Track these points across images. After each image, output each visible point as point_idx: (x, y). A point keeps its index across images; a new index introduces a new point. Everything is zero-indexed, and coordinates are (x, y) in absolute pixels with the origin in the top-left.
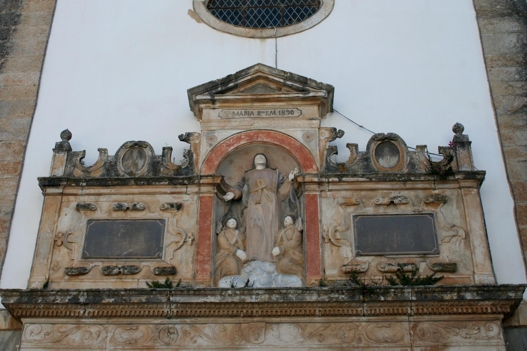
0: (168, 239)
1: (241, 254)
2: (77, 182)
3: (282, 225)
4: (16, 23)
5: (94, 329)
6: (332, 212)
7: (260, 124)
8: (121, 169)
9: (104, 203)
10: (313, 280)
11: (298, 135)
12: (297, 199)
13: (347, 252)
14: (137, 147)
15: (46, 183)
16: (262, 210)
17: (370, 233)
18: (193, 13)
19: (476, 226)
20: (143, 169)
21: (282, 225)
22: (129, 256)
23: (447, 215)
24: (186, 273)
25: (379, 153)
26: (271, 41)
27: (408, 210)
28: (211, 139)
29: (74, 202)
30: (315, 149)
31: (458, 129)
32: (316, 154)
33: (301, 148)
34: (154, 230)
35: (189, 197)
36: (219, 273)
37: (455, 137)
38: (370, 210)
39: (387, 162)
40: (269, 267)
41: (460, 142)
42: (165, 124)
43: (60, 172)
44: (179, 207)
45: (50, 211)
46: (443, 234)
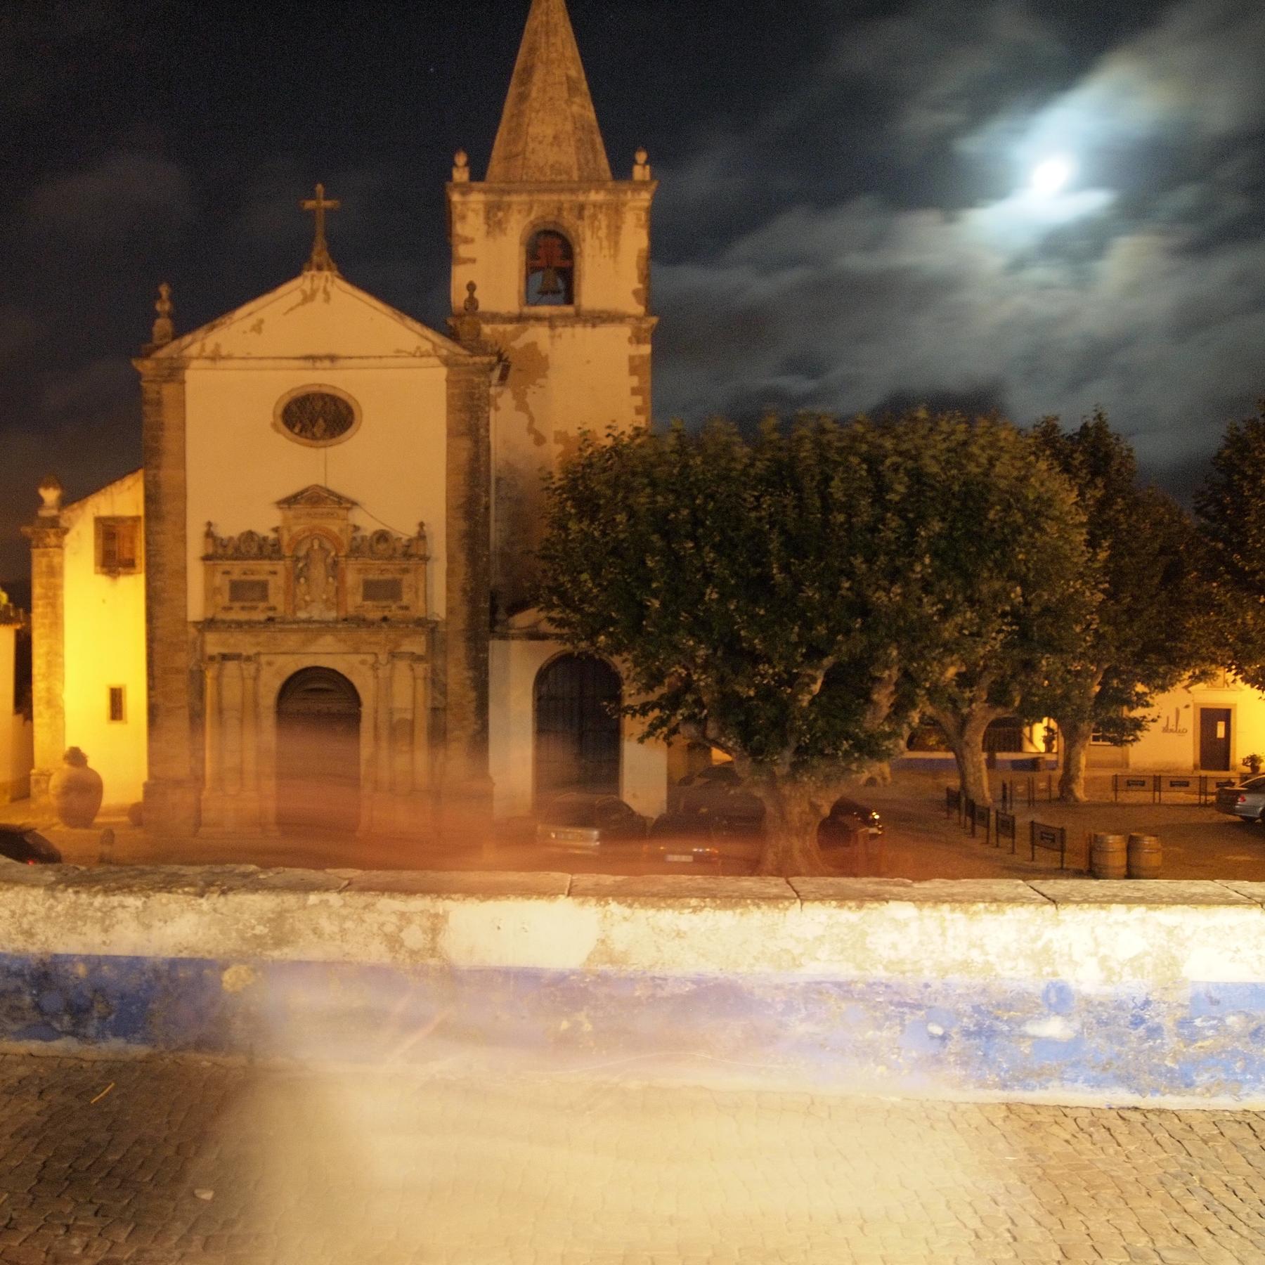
0: (272, 590)
1: (307, 598)
2: (221, 558)
3: (327, 582)
4: (162, 430)
5: (240, 637)
6: (352, 578)
7: (316, 522)
8: (243, 549)
9: (238, 569)
10: (342, 614)
11: (335, 529)
12: (335, 569)
13: (359, 599)
14: (250, 535)
15: (206, 558)
16: (318, 572)
17: (372, 590)
18: (274, 425)
19: (422, 585)
20: (255, 550)
21: (327, 582)
22: (254, 600)
23: (408, 579)
24: (281, 608)
25: (378, 541)
26: (323, 450)
27: (388, 576)
28: (289, 530)
29: (221, 569)
30: (345, 540)
31: (421, 525)
32: (345, 542)
33: (337, 538)
34: (263, 586)
35: (280, 566)
36: (296, 608)
37: (419, 533)
38: (370, 577)
39: (382, 546)
40: (321, 606)
41: (421, 537)
42: (265, 521)
43: (210, 551)
44: (275, 573)
45: (209, 574)
46: (405, 590)
